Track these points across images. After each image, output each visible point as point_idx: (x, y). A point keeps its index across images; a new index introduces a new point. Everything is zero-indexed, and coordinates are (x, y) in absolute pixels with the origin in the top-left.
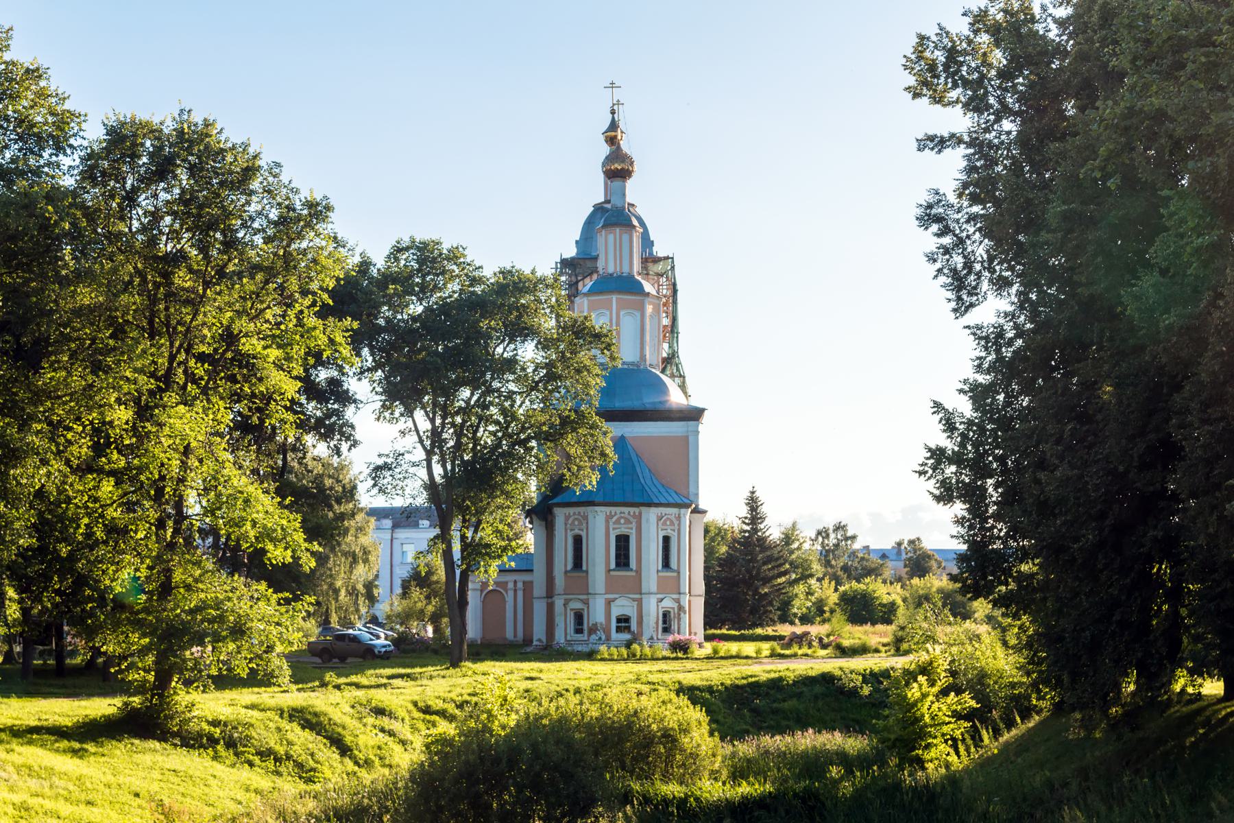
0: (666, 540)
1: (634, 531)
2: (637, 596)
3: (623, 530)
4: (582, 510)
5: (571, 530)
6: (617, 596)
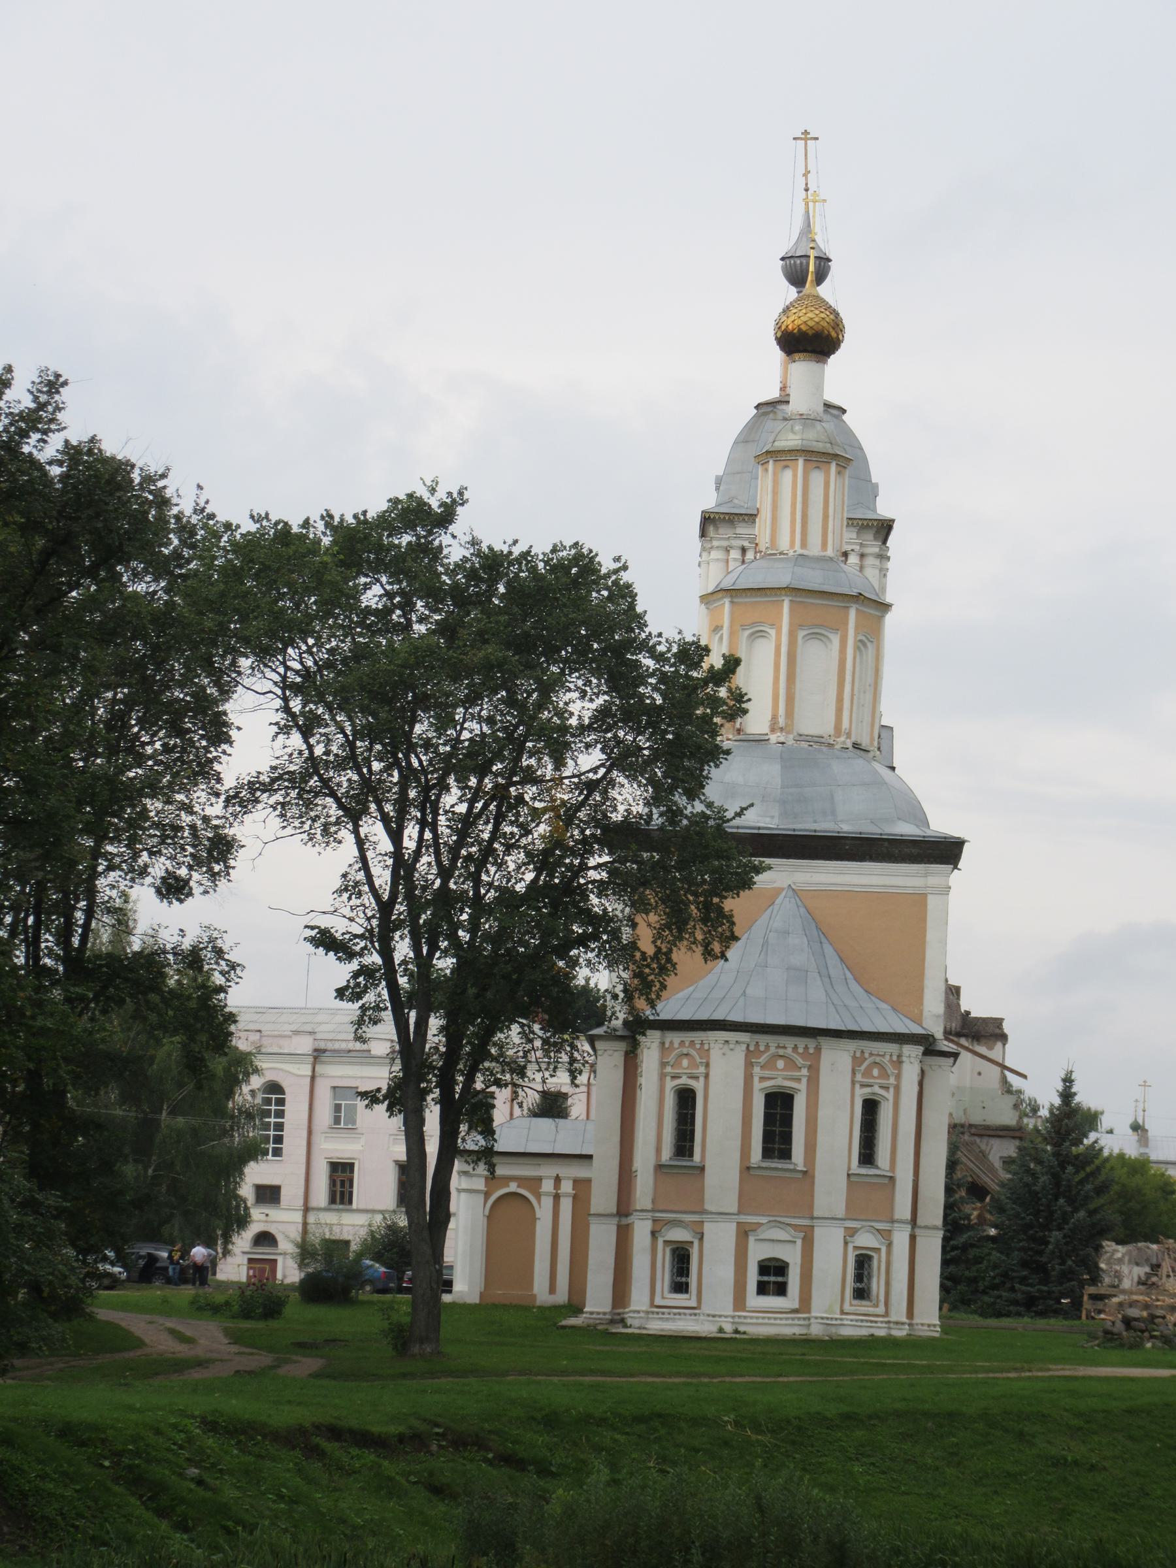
0: (871, 1107)
1: (803, 1086)
3: (780, 1081)
4: (698, 1036)
5: (674, 1077)
6: (764, 1220)
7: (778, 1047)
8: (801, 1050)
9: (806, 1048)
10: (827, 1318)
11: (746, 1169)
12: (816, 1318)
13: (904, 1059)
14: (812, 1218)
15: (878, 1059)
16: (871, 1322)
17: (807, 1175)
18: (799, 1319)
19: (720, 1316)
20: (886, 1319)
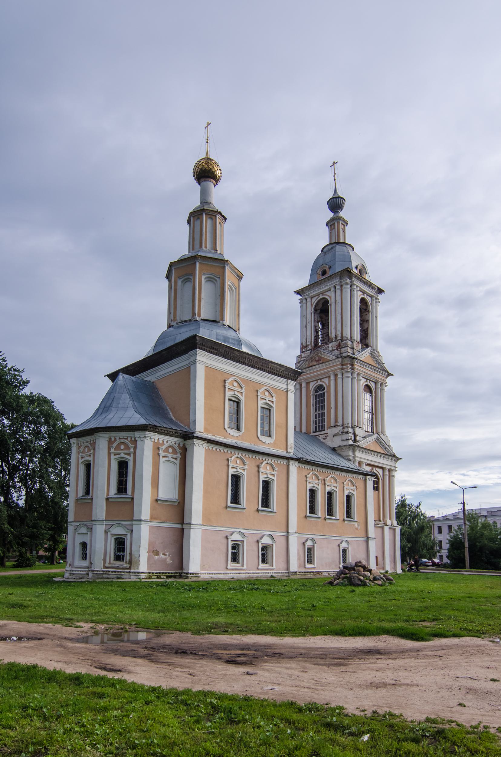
13: (137, 439)
15: (122, 441)
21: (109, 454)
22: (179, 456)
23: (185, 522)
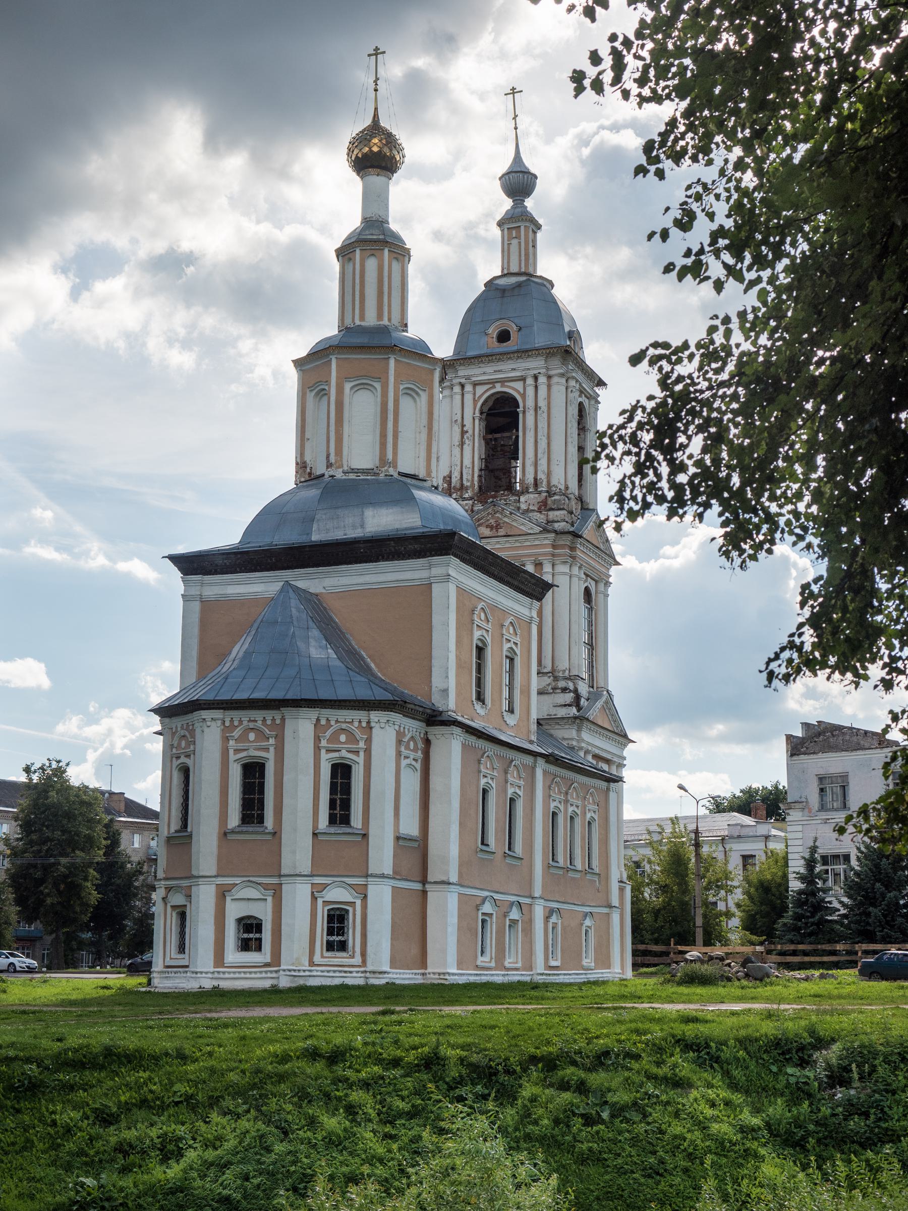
1: (271, 755)
2: (274, 881)
6: (237, 880)
7: (250, 721)
8: (269, 722)
9: (274, 720)
10: (295, 970)
11: (225, 834)
12: (284, 970)
13: (373, 724)
14: (280, 876)
15: (344, 726)
16: (345, 972)
17: (276, 834)
18: (271, 972)
19: (201, 973)
20: (362, 969)
21: (317, 749)
22: (420, 754)
23: (430, 878)
